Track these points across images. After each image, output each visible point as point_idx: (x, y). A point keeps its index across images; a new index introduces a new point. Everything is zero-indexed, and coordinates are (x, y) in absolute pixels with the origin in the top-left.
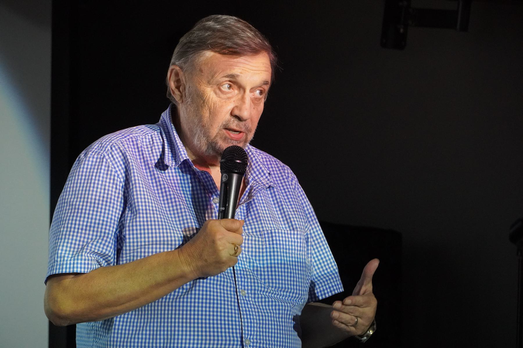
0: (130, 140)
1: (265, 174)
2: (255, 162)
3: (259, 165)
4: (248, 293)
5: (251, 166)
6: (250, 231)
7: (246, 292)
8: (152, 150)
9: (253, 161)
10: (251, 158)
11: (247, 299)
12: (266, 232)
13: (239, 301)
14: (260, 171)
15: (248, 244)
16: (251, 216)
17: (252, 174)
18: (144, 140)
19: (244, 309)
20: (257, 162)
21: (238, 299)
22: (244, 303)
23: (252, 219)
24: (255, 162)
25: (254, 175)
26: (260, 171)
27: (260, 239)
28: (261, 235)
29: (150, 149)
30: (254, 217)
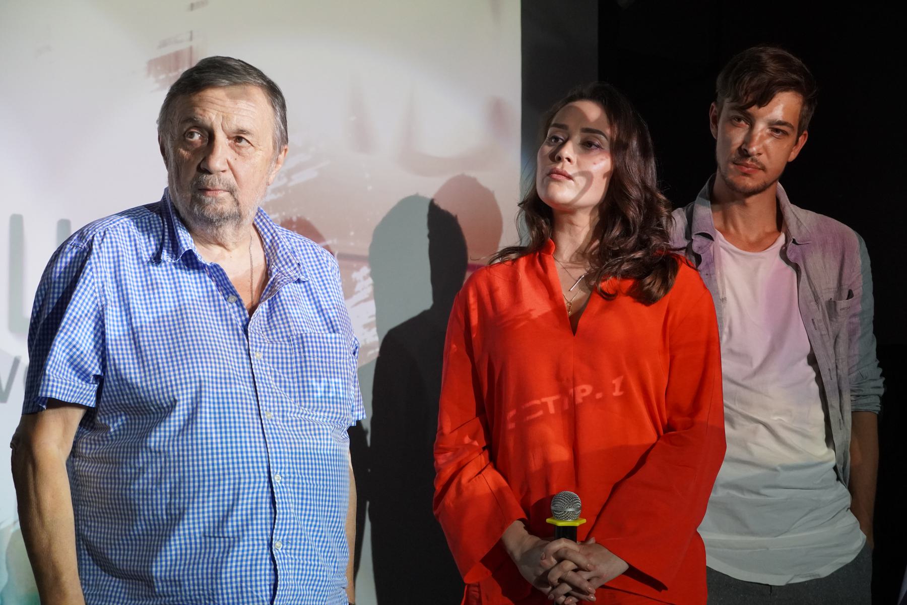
1: (293, 265)
2: (281, 249)
16: (276, 316)
24: (281, 249)
30: (279, 318)
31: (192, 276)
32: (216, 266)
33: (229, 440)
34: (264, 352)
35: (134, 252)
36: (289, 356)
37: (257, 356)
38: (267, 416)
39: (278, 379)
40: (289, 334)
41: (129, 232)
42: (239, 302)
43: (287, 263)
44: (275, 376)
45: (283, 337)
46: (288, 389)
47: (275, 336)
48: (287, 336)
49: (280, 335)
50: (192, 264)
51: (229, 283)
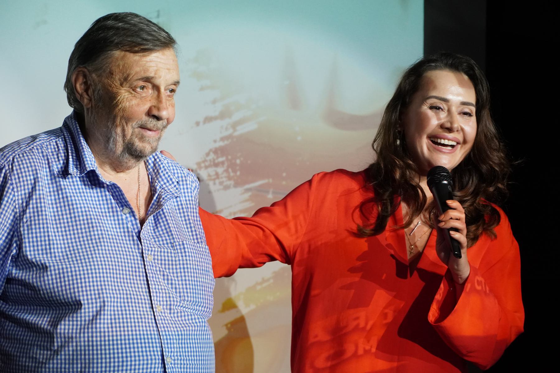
0: (35, 148)
1: (173, 183)
2: (163, 169)
3: (167, 173)
4: (163, 309)
5: (159, 173)
6: (161, 243)
7: (162, 307)
8: (58, 157)
9: (160, 168)
10: (159, 165)
11: (163, 315)
12: (177, 244)
13: (156, 318)
14: (169, 179)
15: (161, 256)
16: (161, 227)
17: (159, 182)
18: (49, 147)
19: (162, 325)
20: (165, 170)
21: (154, 316)
22: (161, 319)
23: (162, 230)
24: (163, 169)
25: (162, 183)
26: (169, 179)
27: (172, 251)
28: (172, 247)
29: (56, 156)
30: (163, 228)
31: (95, 191)
32: (114, 184)
33: (130, 329)
34: (154, 255)
35: (48, 170)
36: (174, 259)
37: (149, 258)
38: (158, 309)
39: (166, 277)
40: (172, 241)
41: (42, 152)
42: (132, 213)
43: (168, 182)
44: (164, 275)
45: (167, 244)
46: (174, 286)
47: (161, 243)
48: (171, 243)
49: (165, 242)
50: (94, 180)
51: (124, 198)
